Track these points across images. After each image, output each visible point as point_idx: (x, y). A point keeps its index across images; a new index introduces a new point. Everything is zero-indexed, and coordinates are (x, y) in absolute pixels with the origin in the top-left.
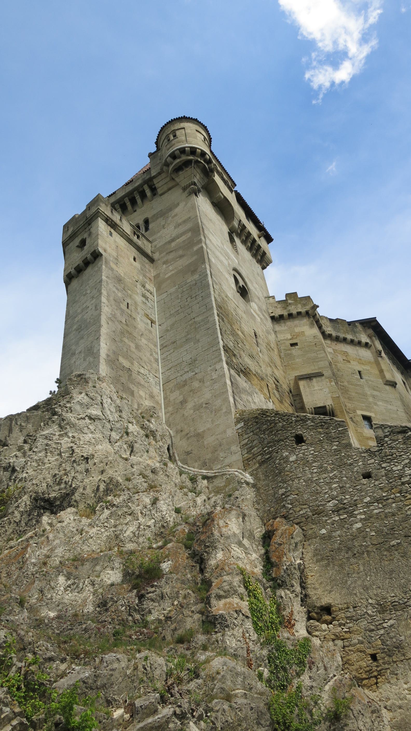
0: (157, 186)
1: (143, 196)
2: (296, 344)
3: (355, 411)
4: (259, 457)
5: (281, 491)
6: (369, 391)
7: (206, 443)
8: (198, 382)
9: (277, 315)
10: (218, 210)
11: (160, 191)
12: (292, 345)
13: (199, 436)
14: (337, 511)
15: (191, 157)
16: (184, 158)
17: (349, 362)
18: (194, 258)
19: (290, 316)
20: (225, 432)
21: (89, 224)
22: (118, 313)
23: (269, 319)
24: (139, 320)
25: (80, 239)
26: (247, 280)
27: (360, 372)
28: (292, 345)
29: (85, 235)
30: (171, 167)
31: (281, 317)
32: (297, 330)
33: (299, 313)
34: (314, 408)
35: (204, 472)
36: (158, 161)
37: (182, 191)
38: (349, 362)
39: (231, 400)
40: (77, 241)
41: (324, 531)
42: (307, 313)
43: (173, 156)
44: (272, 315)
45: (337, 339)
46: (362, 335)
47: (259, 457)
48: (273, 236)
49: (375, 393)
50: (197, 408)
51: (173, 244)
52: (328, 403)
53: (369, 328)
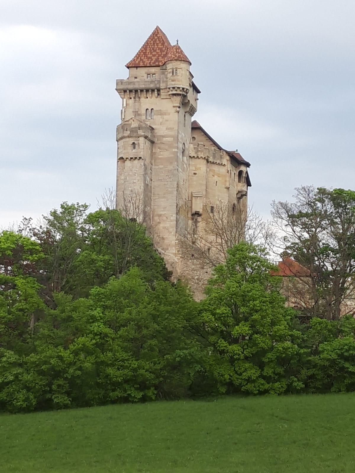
0: (161, 93)
1: (153, 91)
2: (196, 173)
4: (181, 255)
5: (185, 269)
7: (165, 242)
8: (165, 218)
9: (192, 156)
11: (162, 96)
12: (195, 174)
13: (163, 239)
14: (197, 279)
15: (181, 93)
16: (179, 92)
17: (214, 176)
18: (172, 156)
20: (172, 241)
21: (138, 137)
25: (133, 142)
27: (216, 182)
28: (195, 174)
29: (136, 142)
30: (171, 93)
31: (194, 157)
32: (198, 166)
33: (201, 157)
35: (164, 252)
36: (165, 80)
37: (172, 106)
39: (175, 229)
40: (131, 141)
42: (205, 158)
43: (174, 88)
44: (190, 155)
46: (224, 160)
47: (181, 255)
48: (200, 90)
50: (164, 228)
51: (164, 139)
52: (201, 211)
53: (228, 156)
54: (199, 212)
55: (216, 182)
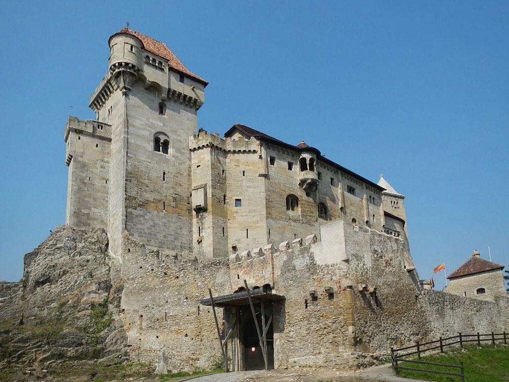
3: (231, 198)
6: (244, 183)
9: (192, 148)
10: (152, 89)
12: (198, 166)
19: (199, 148)
22: (81, 186)
23: (188, 152)
24: (97, 184)
26: (169, 134)
27: (244, 172)
28: (198, 166)
31: (195, 149)
33: (203, 146)
34: (196, 206)
38: (238, 166)
41: (128, 286)
42: (207, 145)
44: (190, 148)
45: (234, 152)
49: (249, 184)
54: (200, 205)
55: (244, 172)
